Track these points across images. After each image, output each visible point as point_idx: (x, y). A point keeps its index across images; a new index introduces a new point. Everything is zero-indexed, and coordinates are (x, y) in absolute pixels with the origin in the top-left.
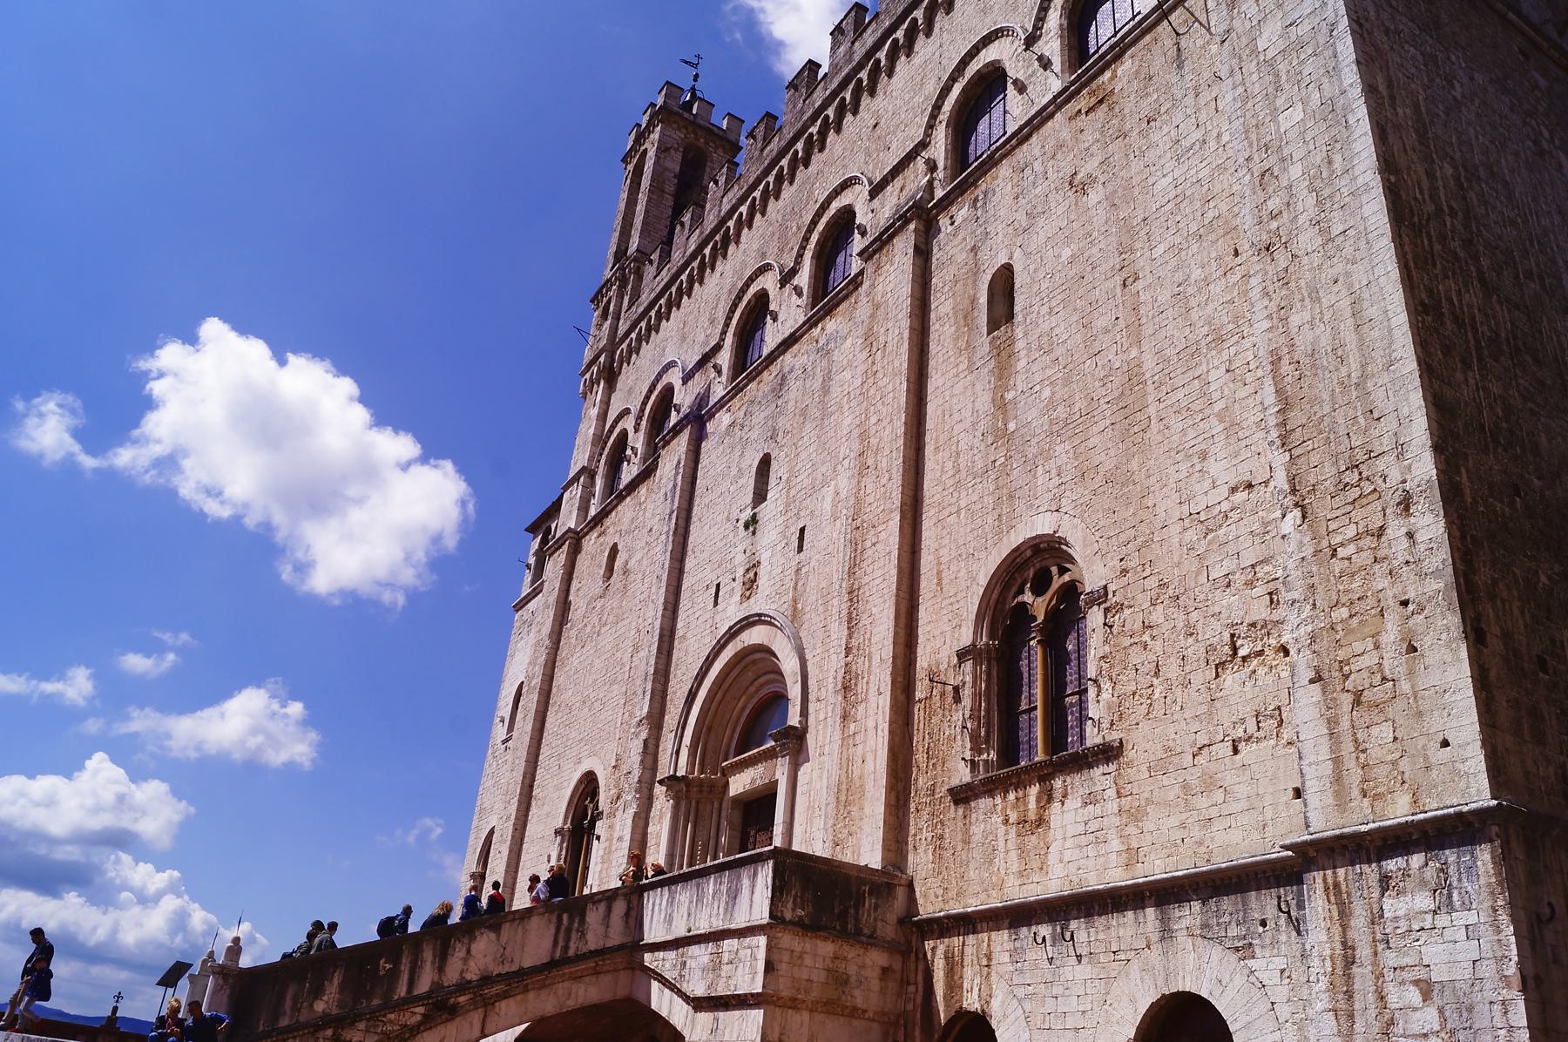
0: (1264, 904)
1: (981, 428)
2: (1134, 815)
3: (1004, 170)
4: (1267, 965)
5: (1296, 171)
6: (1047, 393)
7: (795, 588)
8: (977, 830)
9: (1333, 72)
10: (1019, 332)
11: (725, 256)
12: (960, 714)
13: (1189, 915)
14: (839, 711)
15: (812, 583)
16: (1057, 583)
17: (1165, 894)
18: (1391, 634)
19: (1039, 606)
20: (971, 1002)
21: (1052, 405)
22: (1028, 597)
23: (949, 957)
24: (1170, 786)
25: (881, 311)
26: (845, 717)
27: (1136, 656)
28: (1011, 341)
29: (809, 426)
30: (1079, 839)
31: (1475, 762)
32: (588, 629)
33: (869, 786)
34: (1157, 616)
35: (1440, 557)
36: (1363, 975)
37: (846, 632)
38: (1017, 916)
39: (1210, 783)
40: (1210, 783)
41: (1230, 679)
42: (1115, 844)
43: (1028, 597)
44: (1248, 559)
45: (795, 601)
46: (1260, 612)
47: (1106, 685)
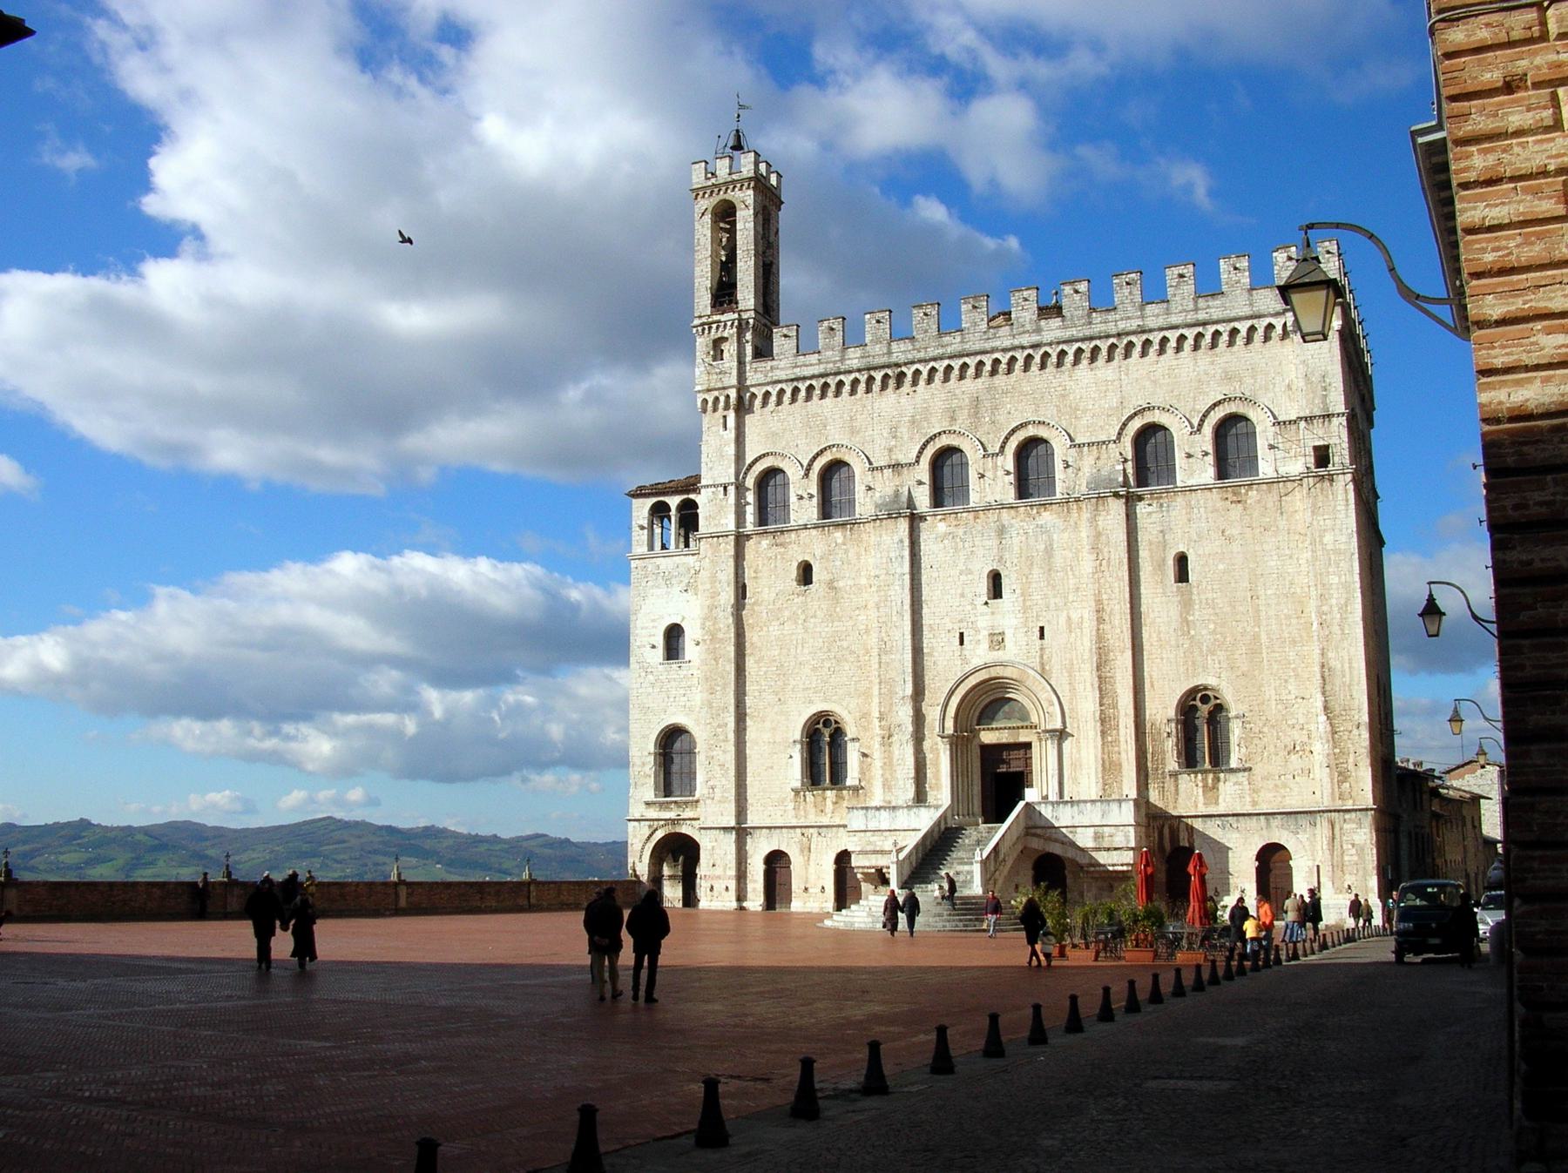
0: (1303, 820)
1: (1174, 625)
3: (1180, 499)
4: (1303, 837)
5: (1334, 601)
6: (1212, 626)
8: (1182, 787)
9: (1351, 572)
10: (1195, 591)
13: (1276, 821)
14: (1099, 728)
16: (1213, 702)
18: (1351, 760)
19: (1204, 710)
21: (1214, 632)
22: (1198, 703)
23: (1171, 828)
24: (1271, 784)
25: (1103, 538)
26: (1103, 733)
27: (1256, 741)
29: (1036, 571)
30: (1231, 793)
33: (1125, 765)
35: (1367, 743)
36: (1337, 841)
39: (1285, 786)
40: (1285, 786)
41: (1293, 757)
42: (1248, 799)
43: (1198, 703)
45: (1042, 664)
46: (1305, 739)
47: (1243, 750)
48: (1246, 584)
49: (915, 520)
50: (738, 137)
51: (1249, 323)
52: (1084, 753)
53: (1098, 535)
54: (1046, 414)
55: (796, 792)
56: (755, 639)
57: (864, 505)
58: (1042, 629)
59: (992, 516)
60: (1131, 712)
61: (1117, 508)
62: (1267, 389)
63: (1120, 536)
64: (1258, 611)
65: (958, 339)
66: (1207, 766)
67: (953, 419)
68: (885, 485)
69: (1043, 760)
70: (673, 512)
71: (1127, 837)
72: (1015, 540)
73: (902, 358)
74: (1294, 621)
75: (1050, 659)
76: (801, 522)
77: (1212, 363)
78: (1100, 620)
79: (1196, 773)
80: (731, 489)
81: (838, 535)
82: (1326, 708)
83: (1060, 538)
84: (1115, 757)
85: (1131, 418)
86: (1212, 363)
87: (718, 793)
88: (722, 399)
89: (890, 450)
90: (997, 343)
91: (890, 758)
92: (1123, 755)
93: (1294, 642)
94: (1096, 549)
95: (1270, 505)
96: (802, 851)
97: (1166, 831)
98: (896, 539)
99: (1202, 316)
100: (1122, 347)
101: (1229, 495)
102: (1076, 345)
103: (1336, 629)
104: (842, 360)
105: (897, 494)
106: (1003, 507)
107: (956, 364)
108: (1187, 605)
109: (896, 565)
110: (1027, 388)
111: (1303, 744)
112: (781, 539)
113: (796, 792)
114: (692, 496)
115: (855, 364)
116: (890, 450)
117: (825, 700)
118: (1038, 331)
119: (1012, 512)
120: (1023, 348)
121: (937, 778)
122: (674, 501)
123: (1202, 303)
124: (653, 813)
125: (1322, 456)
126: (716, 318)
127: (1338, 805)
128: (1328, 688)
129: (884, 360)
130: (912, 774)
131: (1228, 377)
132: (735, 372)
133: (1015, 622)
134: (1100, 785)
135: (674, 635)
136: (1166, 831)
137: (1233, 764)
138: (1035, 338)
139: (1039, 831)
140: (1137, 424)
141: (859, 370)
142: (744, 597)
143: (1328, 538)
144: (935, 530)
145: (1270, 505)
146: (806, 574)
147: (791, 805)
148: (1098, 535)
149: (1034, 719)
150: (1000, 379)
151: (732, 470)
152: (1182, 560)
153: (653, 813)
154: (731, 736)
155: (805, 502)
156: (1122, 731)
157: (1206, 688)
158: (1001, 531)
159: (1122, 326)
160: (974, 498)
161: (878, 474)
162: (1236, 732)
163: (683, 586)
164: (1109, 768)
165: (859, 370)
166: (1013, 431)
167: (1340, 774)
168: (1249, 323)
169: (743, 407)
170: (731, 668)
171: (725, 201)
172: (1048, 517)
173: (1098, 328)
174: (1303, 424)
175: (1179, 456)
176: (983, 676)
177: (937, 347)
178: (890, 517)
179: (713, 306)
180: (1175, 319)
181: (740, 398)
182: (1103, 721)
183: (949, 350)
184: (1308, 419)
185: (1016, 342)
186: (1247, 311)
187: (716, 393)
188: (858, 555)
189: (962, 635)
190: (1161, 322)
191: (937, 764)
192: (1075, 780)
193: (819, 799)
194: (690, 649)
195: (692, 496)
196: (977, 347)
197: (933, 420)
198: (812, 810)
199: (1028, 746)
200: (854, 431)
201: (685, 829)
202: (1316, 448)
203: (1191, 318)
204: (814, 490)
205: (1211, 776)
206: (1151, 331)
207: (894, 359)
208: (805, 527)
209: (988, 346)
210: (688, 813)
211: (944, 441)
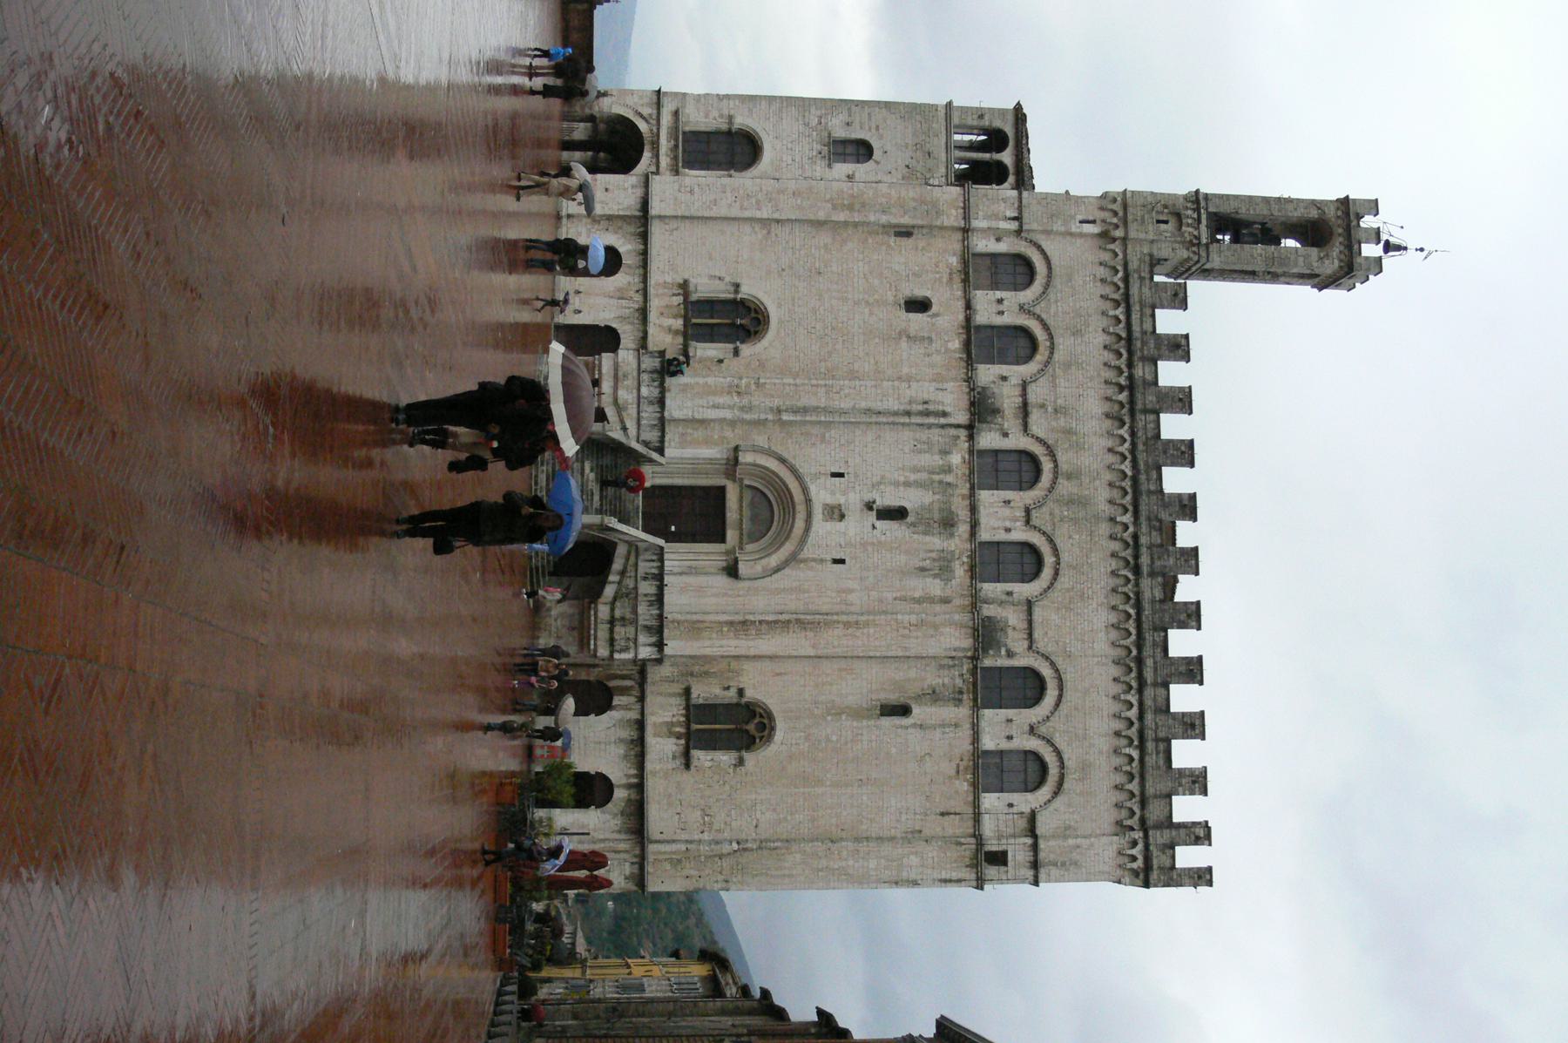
2: (666, 776)
3: (964, 712)
5: (851, 863)
7: (814, 560)
11: (1107, 416)
12: (717, 691)
15: (810, 574)
17: (640, 787)
18: (692, 872)
19: (751, 727)
20: (616, 701)
21: (828, 740)
25: (931, 632)
26: (731, 623)
27: (716, 777)
28: (869, 717)
29: (903, 558)
31: (656, 889)
32: (876, 282)
33: (696, 644)
34: (727, 787)
37: (771, 618)
38: (640, 725)
40: (670, 804)
44: (734, 824)
45: (805, 561)
48: (874, 775)
50: (1399, 248)
51: (1137, 792)
52: (714, 600)
53: (936, 627)
54: (1065, 581)
55: (684, 286)
56: (850, 245)
57: (987, 373)
58: (842, 561)
59: (963, 514)
60: (752, 652)
62: (1069, 805)
64: (846, 785)
65: (1152, 488)
66: (695, 727)
67: (1069, 477)
68: (1008, 398)
69: (708, 554)
70: (997, 156)
71: (626, 649)
73: (1140, 424)
74: (834, 821)
75: (811, 569)
76: (973, 302)
77: (1101, 752)
78: (847, 625)
79: (687, 716)
80: (1014, 226)
81: (956, 344)
82: (745, 850)
84: (705, 634)
85: (1053, 664)
86: (1101, 752)
87: (682, 197)
88: (1115, 220)
89: (1043, 406)
90: (1144, 528)
91: (714, 393)
92: (707, 643)
93: (813, 820)
94: (921, 624)
95: (952, 803)
96: (619, 290)
97: (628, 683)
98: (948, 409)
99: (1150, 746)
101: (964, 763)
102: (1132, 611)
103: (824, 863)
104: (1143, 359)
105: (996, 411)
106: (974, 526)
107: (1127, 484)
108: (858, 713)
109: (920, 408)
110: (1095, 558)
111: (711, 824)
112: (957, 279)
113: (684, 286)
114: (1011, 179)
115: (1139, 372)
116: (1043, 406)
117: (780, 322)
118: (1152, 574)
119: (966, 536)
120: (1136, 557)
121: (696, 443)
122: (1007, 157)
123: (1162, 746)
124: (666, 120)
125: (999, 859)
126: (1204, 217)
127: (651, 858)
128: (765, 852)
129: (1139, 406)
130: (697, 416)
131: (1085, 767)
132: (1142, 236)
133: (852, 532)
134: (679, 617)
135: (863, 150)
136: (628, 683)
137: (695, 753)
138: (1145, 570)
139: (632, 559)
140: (1046, 672)
141: (1131, 377)
142: (899, 234)
143: (914, 860)
145: (952, 803)
146: (919, 305)
147: (669, 279)
148: (936, 627)
149: (749, 547)
150: (1104, 529)
151: (1035, 226)
153: (666, 120)
154: (747, 214)
155: (995, 308)
156: (734, 642)
157: (773, 729)
158: (948, 523)
159: (1149, 662)
160: (984, 496)
161: (1018, 391)
162: (725, 758)
163: (913, 163)
164: (695, 628)
165: (1131, 377)
166: (1051, 541)
167: (679, 861)
168: (1137, 792)
170: (821, 215)
171: (1331, 234)
172: (960, 572)
174: (1029, 841)
175: (1011, 713)
176: (798, 496)
177: (1146, 463)
178: (972, 404)
179: (1215, 214)
180: (1149, 717)
181: (1114, 240)
182: (744, 623)
183: (1143, 477)
184: (1035, 847)
185: (1144, 550)
186: (1150, 790)
187: (1121, 214)
188: (932, 366)
189: (841, 475)
190: (1148, 702)
191: (707, 442)
192: (683, 590)
193: (675, 311)
194: (842, 169)
195: (1011, 179)
196: (1143, 508)
197: (1071, 454)
198: (663, 303)
199: (723, 540)
200: (1067, 366)
201: (647, 155)
202: (1004, 854)
203: (1150, 734)
204: (1007, 319)
205: (682, 730)
206: (1140, 691)
207: (1140, 417)
208: (968, 306)
209: (1143, 519)
210: (665, 161)
211: (1047, 466)
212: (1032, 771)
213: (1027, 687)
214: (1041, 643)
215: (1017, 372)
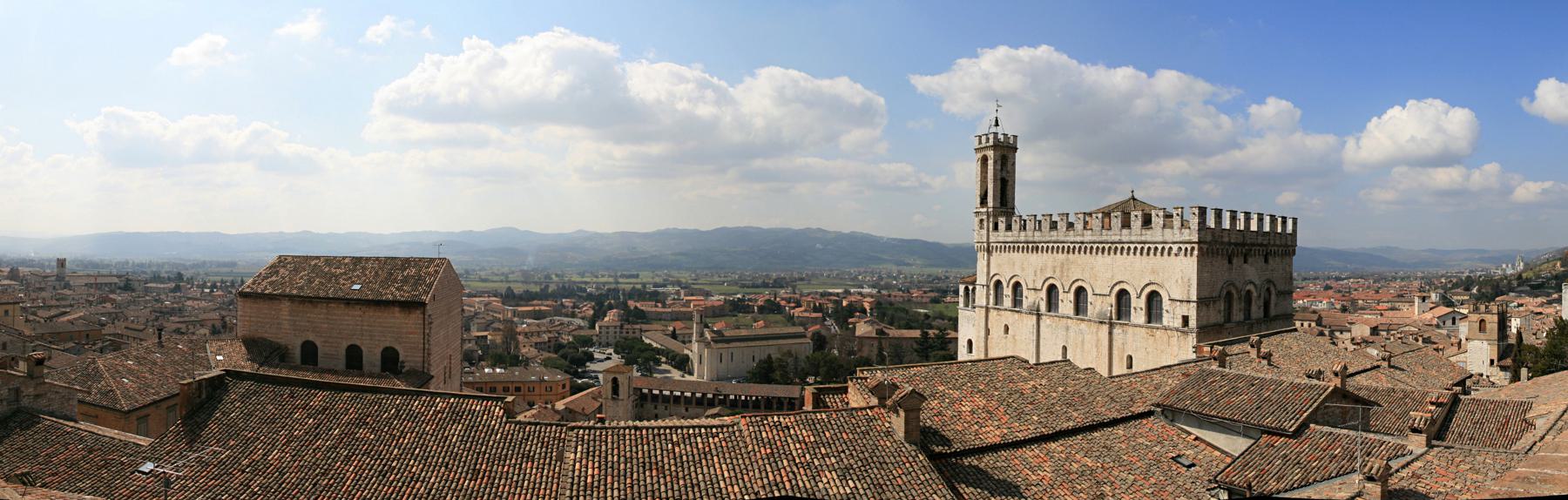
3: (1130, 330)
49: (1039, 316)
54: (1086, 276)
61: (1105, 328)
63: (1106, 343)
72: (1072, 334)
83: (1088, 337)
100: (1114, 248)
125: (1185, 320)
140: (1117, 288)
144: (1046, 321)
146: (1007, 329)
152: (1130, 358)
158: (1067, 328)
169: (989, 252)
172: (1083, 325)
173: (1104, 238)
180: (1133, 239)
212: (1153, 299)
213: (1123, 296)
214: (1107, 291)
215: (1025, 293)
